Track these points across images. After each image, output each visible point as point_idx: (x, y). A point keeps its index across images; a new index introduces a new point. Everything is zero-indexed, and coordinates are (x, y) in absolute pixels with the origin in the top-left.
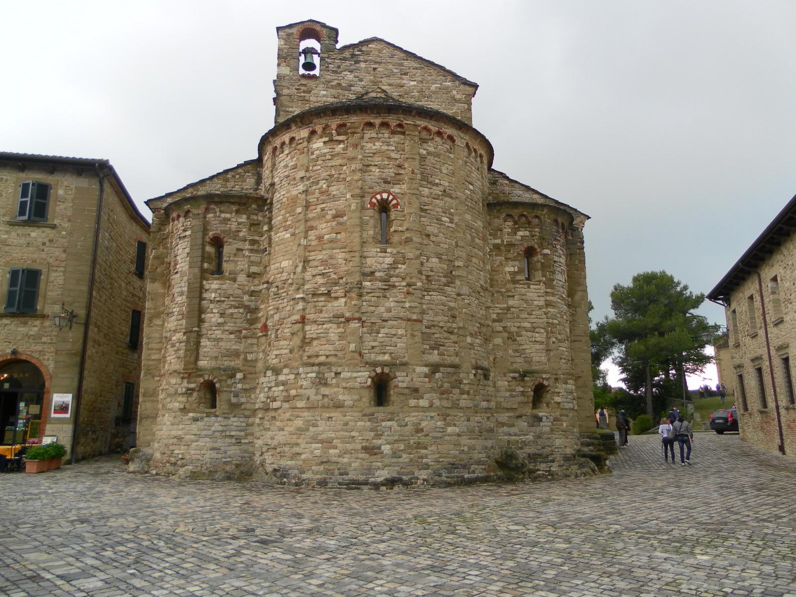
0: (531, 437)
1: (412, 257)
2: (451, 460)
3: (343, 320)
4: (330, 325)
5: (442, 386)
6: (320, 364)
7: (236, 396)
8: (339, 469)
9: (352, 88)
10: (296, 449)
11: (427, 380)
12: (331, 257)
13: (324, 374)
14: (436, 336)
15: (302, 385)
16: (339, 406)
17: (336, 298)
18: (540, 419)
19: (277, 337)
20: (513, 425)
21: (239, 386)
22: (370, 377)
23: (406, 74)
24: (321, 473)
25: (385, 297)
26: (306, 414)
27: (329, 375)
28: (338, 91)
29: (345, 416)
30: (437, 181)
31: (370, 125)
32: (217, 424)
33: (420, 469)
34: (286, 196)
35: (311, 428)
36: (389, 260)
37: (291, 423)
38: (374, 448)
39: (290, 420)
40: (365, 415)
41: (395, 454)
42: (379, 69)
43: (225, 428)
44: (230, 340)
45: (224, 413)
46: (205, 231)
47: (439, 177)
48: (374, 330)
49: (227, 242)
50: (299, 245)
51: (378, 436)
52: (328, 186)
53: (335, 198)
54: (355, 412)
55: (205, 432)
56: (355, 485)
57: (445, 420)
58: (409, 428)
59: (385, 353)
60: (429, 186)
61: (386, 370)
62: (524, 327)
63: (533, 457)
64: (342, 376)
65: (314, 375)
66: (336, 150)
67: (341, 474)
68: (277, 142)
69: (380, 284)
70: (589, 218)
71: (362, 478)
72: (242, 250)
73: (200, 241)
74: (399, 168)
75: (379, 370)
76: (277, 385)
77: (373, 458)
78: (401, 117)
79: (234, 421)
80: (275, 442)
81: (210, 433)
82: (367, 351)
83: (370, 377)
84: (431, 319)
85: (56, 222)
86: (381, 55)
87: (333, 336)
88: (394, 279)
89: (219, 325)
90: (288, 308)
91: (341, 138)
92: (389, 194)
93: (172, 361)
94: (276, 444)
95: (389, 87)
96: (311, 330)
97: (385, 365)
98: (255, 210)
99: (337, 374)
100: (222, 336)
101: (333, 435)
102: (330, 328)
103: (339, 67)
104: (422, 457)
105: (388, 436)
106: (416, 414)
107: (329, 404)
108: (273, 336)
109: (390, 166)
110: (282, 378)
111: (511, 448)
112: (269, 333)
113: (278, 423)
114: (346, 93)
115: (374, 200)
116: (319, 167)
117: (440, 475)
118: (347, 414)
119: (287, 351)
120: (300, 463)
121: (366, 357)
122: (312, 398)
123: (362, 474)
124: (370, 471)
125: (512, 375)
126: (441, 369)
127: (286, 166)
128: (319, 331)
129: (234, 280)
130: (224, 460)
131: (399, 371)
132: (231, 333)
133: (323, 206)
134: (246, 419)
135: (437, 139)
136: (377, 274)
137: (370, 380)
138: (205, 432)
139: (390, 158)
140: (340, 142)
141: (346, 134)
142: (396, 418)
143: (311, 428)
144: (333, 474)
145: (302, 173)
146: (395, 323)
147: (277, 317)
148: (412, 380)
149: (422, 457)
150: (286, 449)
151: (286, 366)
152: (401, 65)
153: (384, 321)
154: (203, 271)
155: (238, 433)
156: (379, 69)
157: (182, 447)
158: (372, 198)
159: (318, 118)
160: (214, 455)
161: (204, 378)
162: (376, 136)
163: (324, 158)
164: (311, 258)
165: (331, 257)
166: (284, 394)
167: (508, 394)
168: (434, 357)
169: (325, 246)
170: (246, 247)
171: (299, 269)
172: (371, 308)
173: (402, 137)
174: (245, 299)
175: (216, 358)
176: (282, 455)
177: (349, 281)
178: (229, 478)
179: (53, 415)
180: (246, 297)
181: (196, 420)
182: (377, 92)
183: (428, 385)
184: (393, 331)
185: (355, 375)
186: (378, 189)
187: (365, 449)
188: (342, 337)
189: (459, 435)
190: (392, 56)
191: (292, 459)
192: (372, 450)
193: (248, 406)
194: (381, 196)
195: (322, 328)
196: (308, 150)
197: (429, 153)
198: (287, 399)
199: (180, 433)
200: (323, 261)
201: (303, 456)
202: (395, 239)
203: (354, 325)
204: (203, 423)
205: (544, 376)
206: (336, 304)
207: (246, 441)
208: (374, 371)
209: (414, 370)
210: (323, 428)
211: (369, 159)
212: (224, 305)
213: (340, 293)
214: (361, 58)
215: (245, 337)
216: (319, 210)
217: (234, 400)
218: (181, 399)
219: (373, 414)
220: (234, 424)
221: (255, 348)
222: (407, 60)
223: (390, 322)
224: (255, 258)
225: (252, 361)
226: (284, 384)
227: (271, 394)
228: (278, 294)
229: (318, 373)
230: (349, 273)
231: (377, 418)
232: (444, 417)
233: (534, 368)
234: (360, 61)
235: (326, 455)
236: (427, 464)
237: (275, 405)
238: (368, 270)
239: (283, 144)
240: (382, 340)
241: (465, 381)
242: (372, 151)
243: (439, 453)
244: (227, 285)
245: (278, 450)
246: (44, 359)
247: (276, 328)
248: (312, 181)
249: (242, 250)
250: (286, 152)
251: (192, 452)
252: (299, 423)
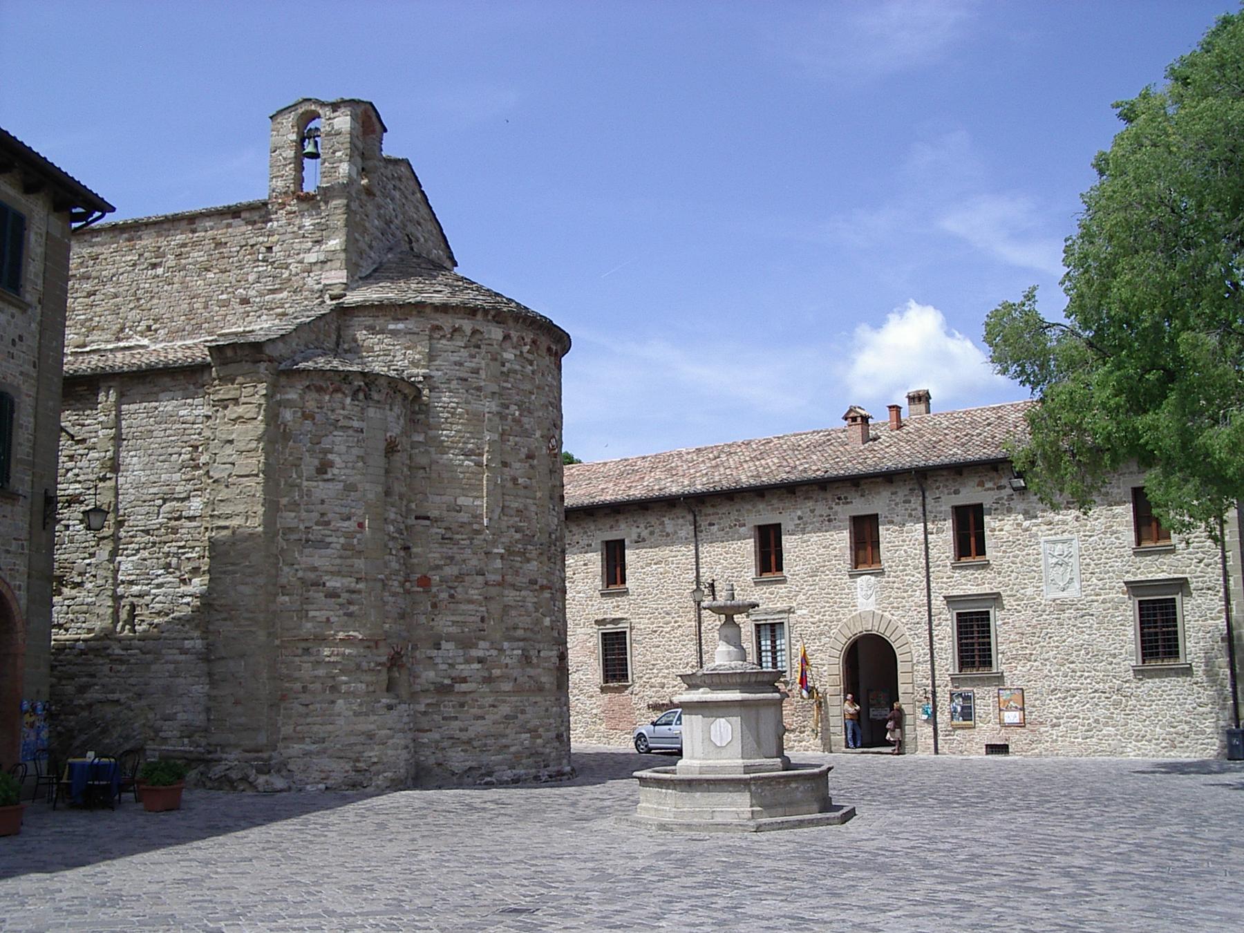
3: (537, 587)
10: (504, 741)
16: (540, 689)
19: (452, 596)
27: (533, 653)
35: (519, 715)
37: (495, 710)
39: (494, 706)
68: (447, 322)
76: (468, 661)
80: (471, 733)
90: (474, 562)
93: (332, 619)
94: (473, 736)
108: (444, 595)
110: (475, 653)
112: (434, 590)
116: (510, 386)
120: (509, 757)
122: (520, 679)
133: (517, 439)
143: (519, 715)
147: (451, 571)
150: (490, 741)
151: (479, 639)
157: (376, 748)
166: (486, 674)
176: (484, 749)
181: (390, 707)
191: (498, 753)
198: (488, 680)
199: (372, 727)
200: (518, 511)
201: (512, 749)
213: (534, 554)
218: (368, 678)
227: (454, 673)
228: (450, 539)
245: (475, 744)
247: (450, 584)
252: (505, 709)
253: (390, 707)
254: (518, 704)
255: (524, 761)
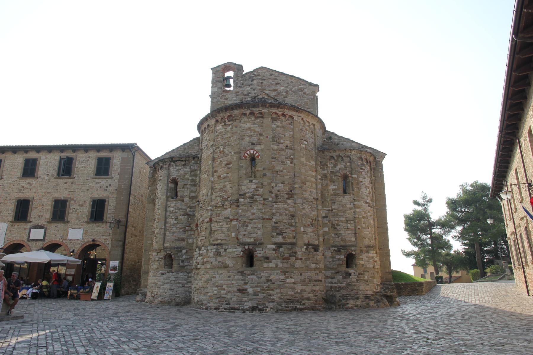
0: (345, 285)
1: (266, 184)
2: (289, 297)
4: (223, 223)
5: (284, 256)
6: (217, 245)
7: (182, 261)
8: (226, 301)
9: (250, 94)
10: (207, 290)
11: (274, 252)
12: (224, 186)
13: (219, 250)
14: (281, 227)
15: (209, 256)
16: (226, 267)
17: (226, 209)
18: (350, 274)
20: (334, 278)
21: (184, 257)
22: (242, 251)
23: (279, 84)
24: (217, 304)
25: (251, 206)
26: (211, 271)
27: (222, 250)
28: (242, 97)
29: (229, 272)
30: (282, 141)
31: (245, 114)
32: (172, 276)
33: (269, 302)
34: (206, 155)
35: (213, 279)
36: (254, 187)
38: (243, 290)
39: (204, 274)
40: (239, 272)
41: (255, 294)
42: (264, 83)
43: (176, 279)
44: (180, 232)
45: (176, 271)
46: (169, 175)
47: (283, 139)
48: (245, 225)
49: (179, 181)
50: (210, 181)
51: (246, 283)
52: (223, 149)
53: (227, 155)
54: (233, 270)
55: (167, 281)
56: (233, 310)
57: (285, 274)
58: (264, 279)
59: (251, 238)
60: (277, 144)
61: (251, 247)
62: (340, 221)
63: (345, 297)
64: (228, 251)
65: (215, 250)
66: (228, 129)
67: (227, 304)
69: (249, 200)
70: (386, 154)
71: (236, 306)
72: (187, 185)
73: (166, 182)
74: (260, 136)
75: (247, 247)
77: (243, 296)
78: (261, 108)
79: (181, 275)
81: (169, 281)
82: (241, 237)
83: (242, 251)
84: (278, 218)
85: (113, 175)
86: (265, 75)
87: (224, 229)
88: (256, 197)
89: (174, 224)
91: (230, 123)
92: (254, 150)
95: (269, 92)
96: (214, 226)
97: (251, 245)
98: (194, 163)
99: (226, 250)
100: (176, 231)
101: (223, 283)
102: (223, 225)
103: (243, 84)
104: (270, 295)
105: (251, 283)
106: (268, 271)
107: (221, 265)
109: (255, 135)
110: (201, 252)
111: (333, 291)
113: (200, 276)
114: (246, 97)
115: (246, 155)
116: (220, 139)
117: (281, 306)
118: (230, 271)
119: (204, 238)
120: (208, 297)
121: (241, 241)
122: (214, 263)
123: (237, 304)
124: (241, 302)
125: (334, 248)
126: (284, 246)
127: (206, 140)
128: (217, 227)
129: (183, 201)
130: (176, 295)
131: (258, 247)
132: (181, 229)
133: (221, 159)
134: (188, 274)
135: (283, 118)
136: (247, 195)
137: (242, 253)
138: (167, 281)
139: (254, 131)
140: (230, 125)
141: (232, 120)
142: (256, 274)
143: (213, 279)
144: (223, 304)
145: (211, 143)
146: (256, 221)
148: (265, 252)
149: (270, 295)
151: (203, 246)
152: (276, 79)
153: (252, 220)
154: (167, 197)
155: (183, 282)
156: (264, 83)
157: (157, 288)
158: (245, 153)
159: (219, 113)
160: (171, 292)
161: (167, 253)
162: (247, 120)
163: (222, 134)
164: (215, 187)
165: (224, 186)
166: (202, 261)
167: (331, 260)
168: (280, 239)
169: (221, 181)
170: (189, 183)
171: (209, 194)
172: (244, 213)
173: (262, 119)
174: (188, 210)
175: (173, 242)
177: (232, 199)
178: (177, 305)
179: (110, 272)
180: (188, 209)
181: (163, 274)
182: (263, 95)
183: (276, 255)
184: (255, 226)
185: (234, 250)
186: (248, 148)
187: (240, 291)
188: (229, 230)
189: (294, 283)
190: (271, 75)
192: (242, 291)
193: (189, 267)
194: (250, 152)
195: (219, 225)
196: (215, 130)
197: (278, 127)
199: (156, 281)
201: (209, 294)
202: (258, 174)
203: (234, 223)
204: (166, 276)
205: (353, 249)
206: (226, 212)
207: (187, 286)
208: (244, 248)
209: (266, 247)
210: (219, 279)
211: (244, 132)
212: (177, 215)
213: (228, 206)
214: (255, 78)
215: (188, 231)
216: (219, 162)
217: (181, 264)
218: (157, 263)
219: (243, 272)
220: (181, 277)
221: (193, 236)
222: (279, 76)
223: (254, 221)
224: (193, 188)
225: (191, 243)
226: (202, 255)
229: (217, 249)
230: (232, 194)
231: (245, 274)
232: (285, 273)
233: (347, 244)
234: (254, 80)
235: (220, 293)
236: (274, 299)
237: (199, 266)
238: (242, 193)
239: (205, 128)
240: (249, 231)
241: (299, 253)
242: (245, 128)
243: (281, 293)
244: (179, 204)
246: (106, 244)
248: (216, 146)
249: (187, 185)
250: (207, 132)
251: (161, 291)
252: (208, 276)
253: (163, 274)
254: (212, 273)
255: (214, 300)
